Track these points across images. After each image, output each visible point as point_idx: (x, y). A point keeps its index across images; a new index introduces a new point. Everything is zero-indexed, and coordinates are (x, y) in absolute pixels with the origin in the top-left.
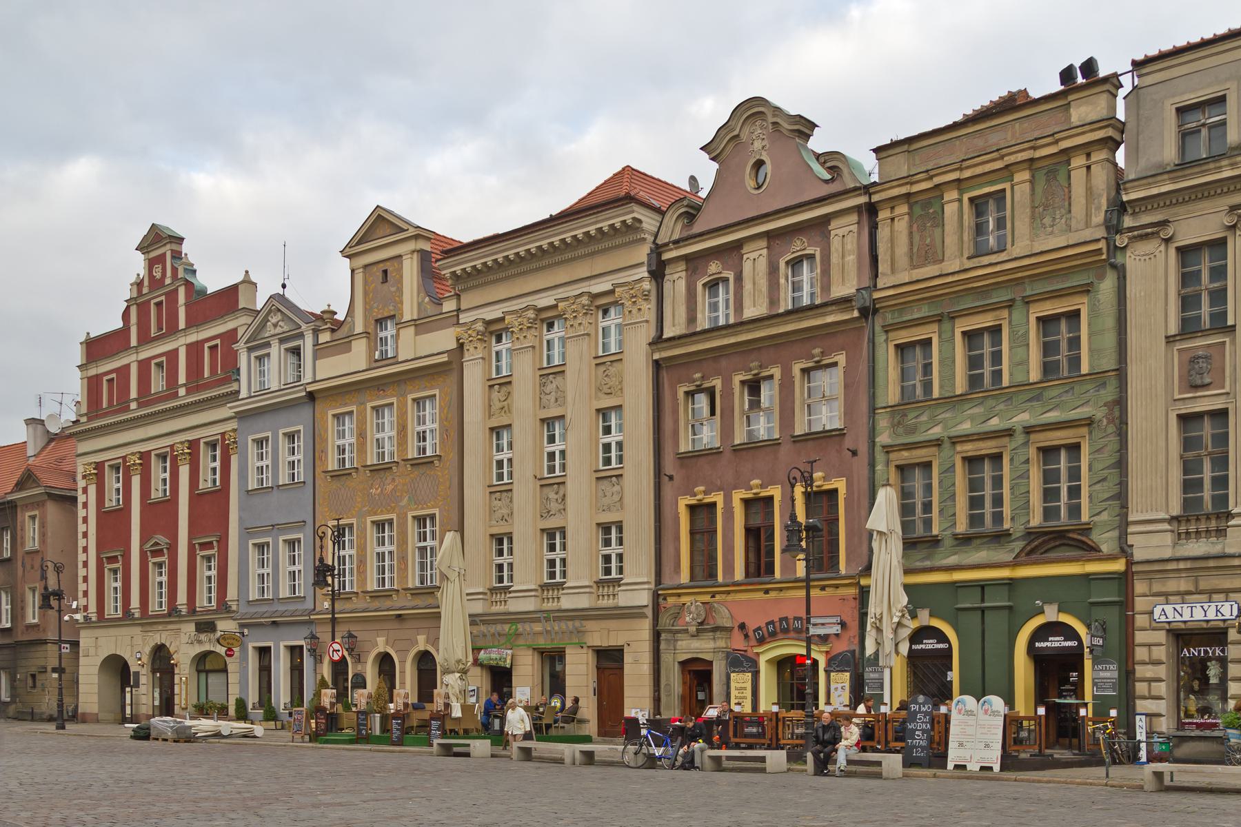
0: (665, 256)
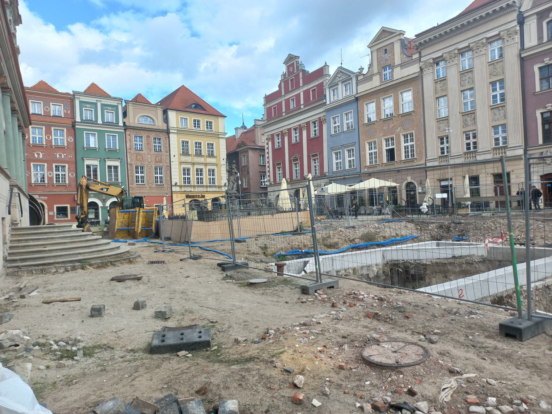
0: (525, 15)
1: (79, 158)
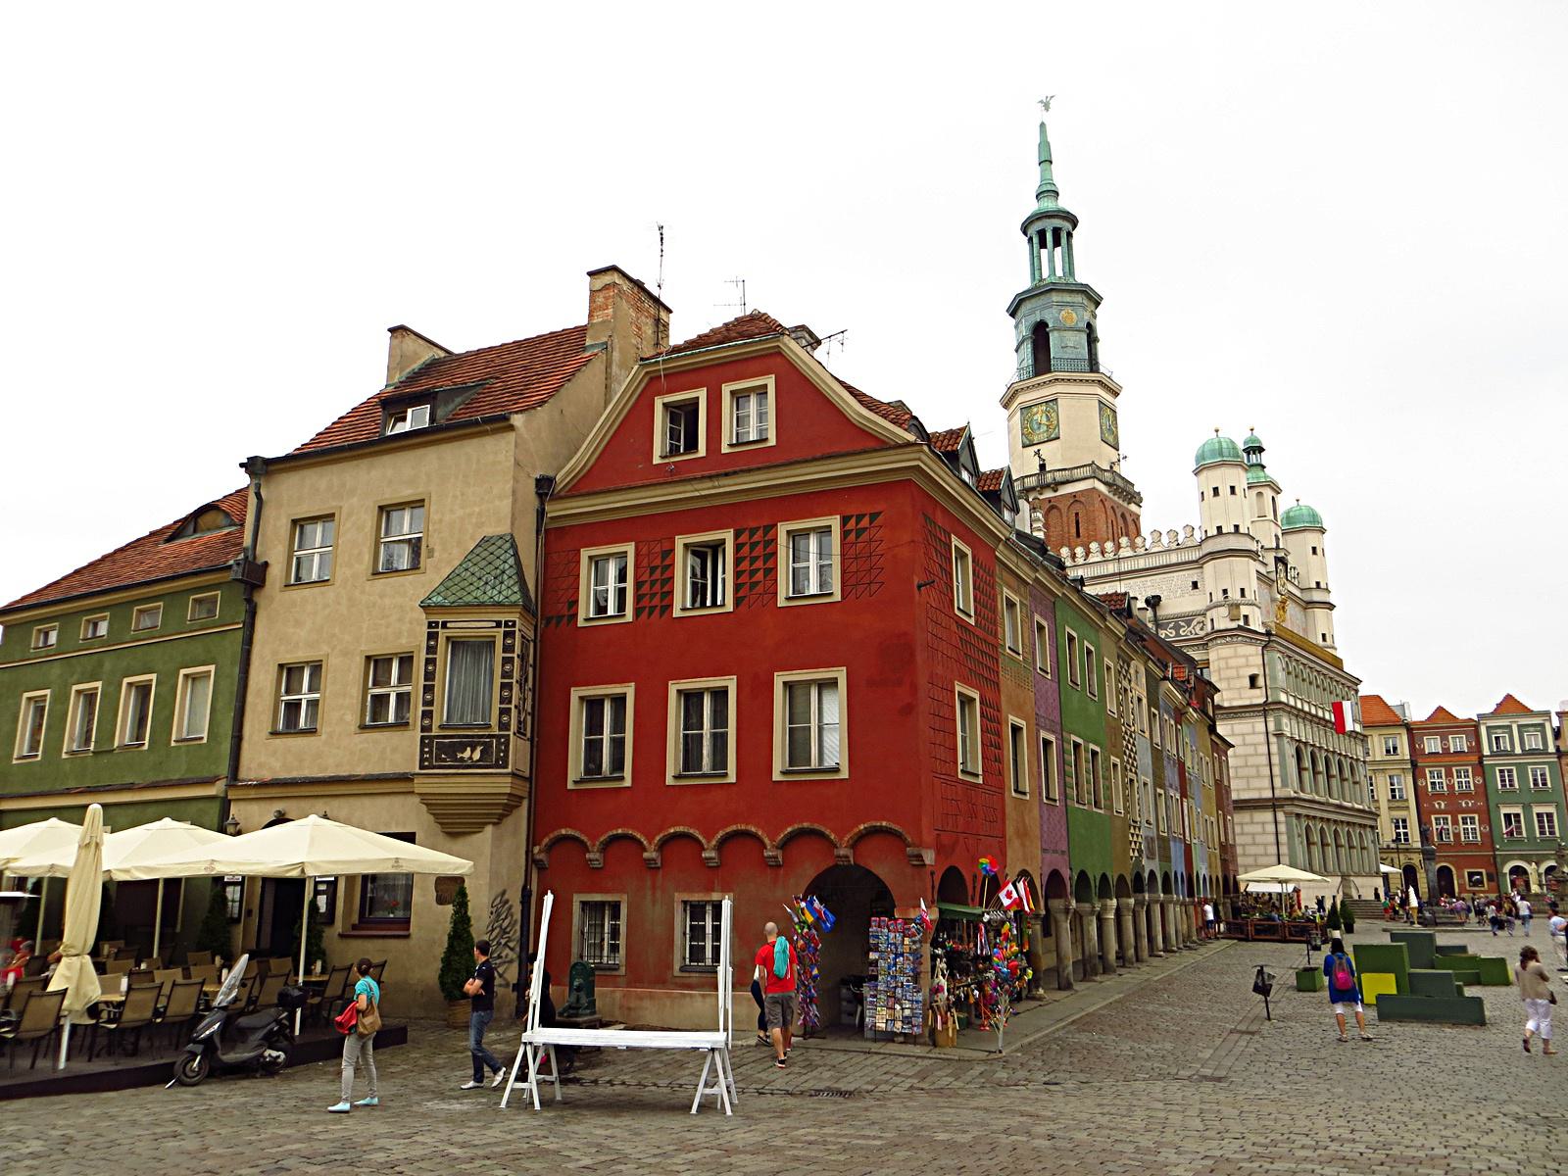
1: (1492, 805)
